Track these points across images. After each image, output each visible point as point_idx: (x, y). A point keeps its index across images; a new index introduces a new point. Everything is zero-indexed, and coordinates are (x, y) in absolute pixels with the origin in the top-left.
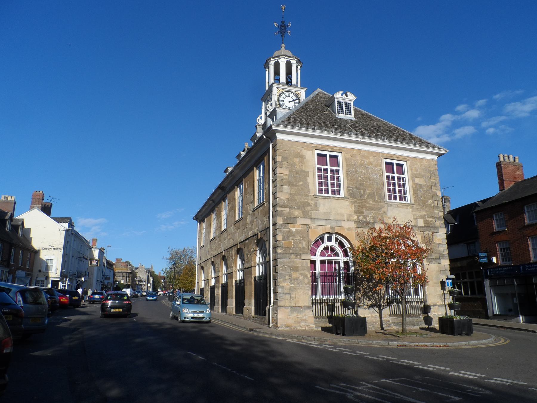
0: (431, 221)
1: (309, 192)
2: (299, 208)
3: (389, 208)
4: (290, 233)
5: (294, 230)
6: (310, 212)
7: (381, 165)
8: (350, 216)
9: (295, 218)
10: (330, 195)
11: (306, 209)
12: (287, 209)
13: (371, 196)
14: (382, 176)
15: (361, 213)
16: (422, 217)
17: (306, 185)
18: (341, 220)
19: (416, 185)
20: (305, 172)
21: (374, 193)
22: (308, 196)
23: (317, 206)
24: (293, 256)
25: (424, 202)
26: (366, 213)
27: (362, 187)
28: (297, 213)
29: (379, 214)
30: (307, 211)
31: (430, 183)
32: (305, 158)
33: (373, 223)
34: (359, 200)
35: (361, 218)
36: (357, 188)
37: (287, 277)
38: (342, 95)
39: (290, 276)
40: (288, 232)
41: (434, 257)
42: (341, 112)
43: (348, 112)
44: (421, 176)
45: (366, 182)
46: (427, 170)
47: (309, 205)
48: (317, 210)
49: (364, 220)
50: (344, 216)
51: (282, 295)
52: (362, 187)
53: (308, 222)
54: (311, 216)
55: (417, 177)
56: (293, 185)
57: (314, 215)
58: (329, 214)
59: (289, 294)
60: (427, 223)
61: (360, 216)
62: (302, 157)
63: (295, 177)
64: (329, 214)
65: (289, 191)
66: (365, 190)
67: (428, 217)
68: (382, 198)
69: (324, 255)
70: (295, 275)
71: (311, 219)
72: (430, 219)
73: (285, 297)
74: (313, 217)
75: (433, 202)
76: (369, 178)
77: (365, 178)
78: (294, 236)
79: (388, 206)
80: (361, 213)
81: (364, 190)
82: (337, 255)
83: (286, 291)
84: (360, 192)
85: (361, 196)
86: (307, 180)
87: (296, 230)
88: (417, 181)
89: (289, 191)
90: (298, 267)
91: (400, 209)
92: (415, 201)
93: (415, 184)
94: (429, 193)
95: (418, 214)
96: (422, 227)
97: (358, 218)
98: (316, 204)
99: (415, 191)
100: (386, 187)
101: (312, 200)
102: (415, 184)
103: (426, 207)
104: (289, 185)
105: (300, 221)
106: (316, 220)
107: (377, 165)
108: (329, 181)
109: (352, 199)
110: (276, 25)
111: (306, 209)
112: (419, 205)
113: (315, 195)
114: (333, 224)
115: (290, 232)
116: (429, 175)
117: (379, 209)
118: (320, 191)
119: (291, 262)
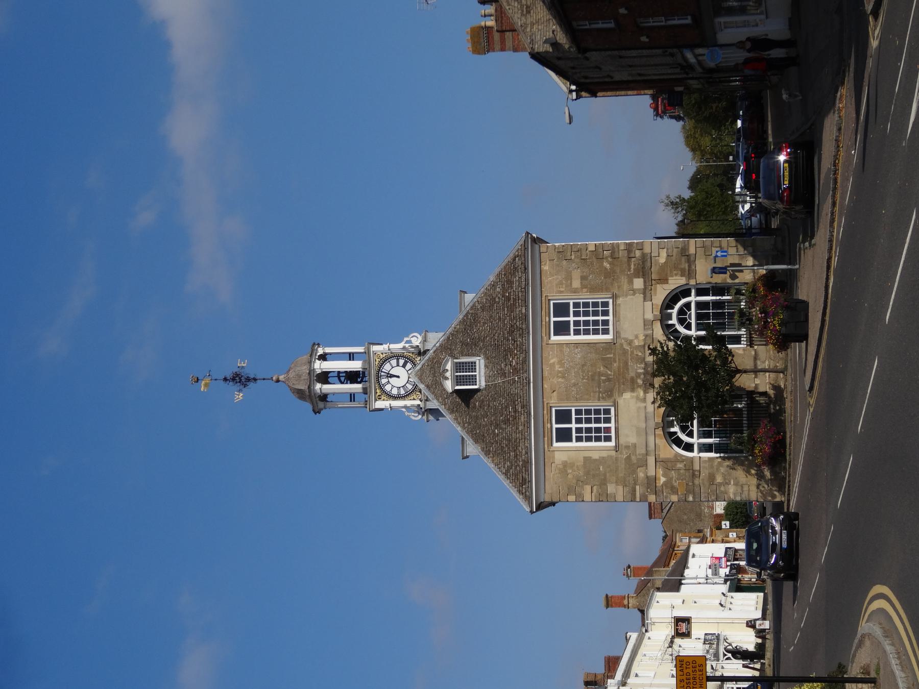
1: (611, 457)
2: (634, 472)
3: (623, 335)
5: (663, 480)
7: (560, 345)
8: (638, 398)
9: (647, 477)
10: (612, 425)
12: (638, 487)
13: (607, 363)
14: (577, 345)
15: (633, 381)
16: (631, 282)
17: (602, 460)
19: (583, 286)
21: (603, 359)
22: (617, 459)
24: (697, 482)
25: (608, 274)
27: (597, 378)
28: (641, 475)
29: (632, 352)
30: (638, 460)
31: (578, 260)
32: (566, 462)
33: (646, 364)
35: (640, 382)
36: (599, 387)
37: (722, 489)
38: (447, 378)
39: (720, 484)
40: (667, 487)
41: (687, 265)
42: (472, 380)
43: (472, 366)
44: (569, 277)
45: (588, 371)
46: (558, 265)
47: (629, 458)
48: (635, 446)
49: (642, 376)
50: (639, 408)
51: (743, 496)
52: (597, 378)
53: (651, 460)
55: (571, 284)
56: (605, 479)
57: (641, 450)
58: (638, 429)
59: (742, 487)
62: (565, 464)
63: (594, 476)
64: (638, 429)
67: (629, 270)
68: (609, 346)
69: (692, 431)
70: (719, 479)
72: (632, 266)
73: (746, 493)
74: (644, 451)
75: (607, 258)
76: (583, 366)
77: (583, 372)
80: (633, 381)
81: (600, 374)
83: (739, 490)
84: (604, 381)
85: (609, 380)
87: (663, 476)
88: (576, 284)
89: (614, 485)
91: (621, 319)
92: (607, 290)
93: (582, 288)
94: (592, 263)
95: (626, 287)
96: (645, 282)
97: (639, 386)
98: (627, 447)
99: (593, 289)
100: (591, 337)
101: (621, 453)
102: (582, 288)
103: (614, 272)
104: (605, 484)
105: (651, 473)
106: (649, 449)
108: (593, 425)
109: (616, 394)
112: (612, 284)
113: (617, 448)
114: (652, 424)
115: (665, 484)
116: (564, 262)
117: (625, 352)
118: (608, 439)
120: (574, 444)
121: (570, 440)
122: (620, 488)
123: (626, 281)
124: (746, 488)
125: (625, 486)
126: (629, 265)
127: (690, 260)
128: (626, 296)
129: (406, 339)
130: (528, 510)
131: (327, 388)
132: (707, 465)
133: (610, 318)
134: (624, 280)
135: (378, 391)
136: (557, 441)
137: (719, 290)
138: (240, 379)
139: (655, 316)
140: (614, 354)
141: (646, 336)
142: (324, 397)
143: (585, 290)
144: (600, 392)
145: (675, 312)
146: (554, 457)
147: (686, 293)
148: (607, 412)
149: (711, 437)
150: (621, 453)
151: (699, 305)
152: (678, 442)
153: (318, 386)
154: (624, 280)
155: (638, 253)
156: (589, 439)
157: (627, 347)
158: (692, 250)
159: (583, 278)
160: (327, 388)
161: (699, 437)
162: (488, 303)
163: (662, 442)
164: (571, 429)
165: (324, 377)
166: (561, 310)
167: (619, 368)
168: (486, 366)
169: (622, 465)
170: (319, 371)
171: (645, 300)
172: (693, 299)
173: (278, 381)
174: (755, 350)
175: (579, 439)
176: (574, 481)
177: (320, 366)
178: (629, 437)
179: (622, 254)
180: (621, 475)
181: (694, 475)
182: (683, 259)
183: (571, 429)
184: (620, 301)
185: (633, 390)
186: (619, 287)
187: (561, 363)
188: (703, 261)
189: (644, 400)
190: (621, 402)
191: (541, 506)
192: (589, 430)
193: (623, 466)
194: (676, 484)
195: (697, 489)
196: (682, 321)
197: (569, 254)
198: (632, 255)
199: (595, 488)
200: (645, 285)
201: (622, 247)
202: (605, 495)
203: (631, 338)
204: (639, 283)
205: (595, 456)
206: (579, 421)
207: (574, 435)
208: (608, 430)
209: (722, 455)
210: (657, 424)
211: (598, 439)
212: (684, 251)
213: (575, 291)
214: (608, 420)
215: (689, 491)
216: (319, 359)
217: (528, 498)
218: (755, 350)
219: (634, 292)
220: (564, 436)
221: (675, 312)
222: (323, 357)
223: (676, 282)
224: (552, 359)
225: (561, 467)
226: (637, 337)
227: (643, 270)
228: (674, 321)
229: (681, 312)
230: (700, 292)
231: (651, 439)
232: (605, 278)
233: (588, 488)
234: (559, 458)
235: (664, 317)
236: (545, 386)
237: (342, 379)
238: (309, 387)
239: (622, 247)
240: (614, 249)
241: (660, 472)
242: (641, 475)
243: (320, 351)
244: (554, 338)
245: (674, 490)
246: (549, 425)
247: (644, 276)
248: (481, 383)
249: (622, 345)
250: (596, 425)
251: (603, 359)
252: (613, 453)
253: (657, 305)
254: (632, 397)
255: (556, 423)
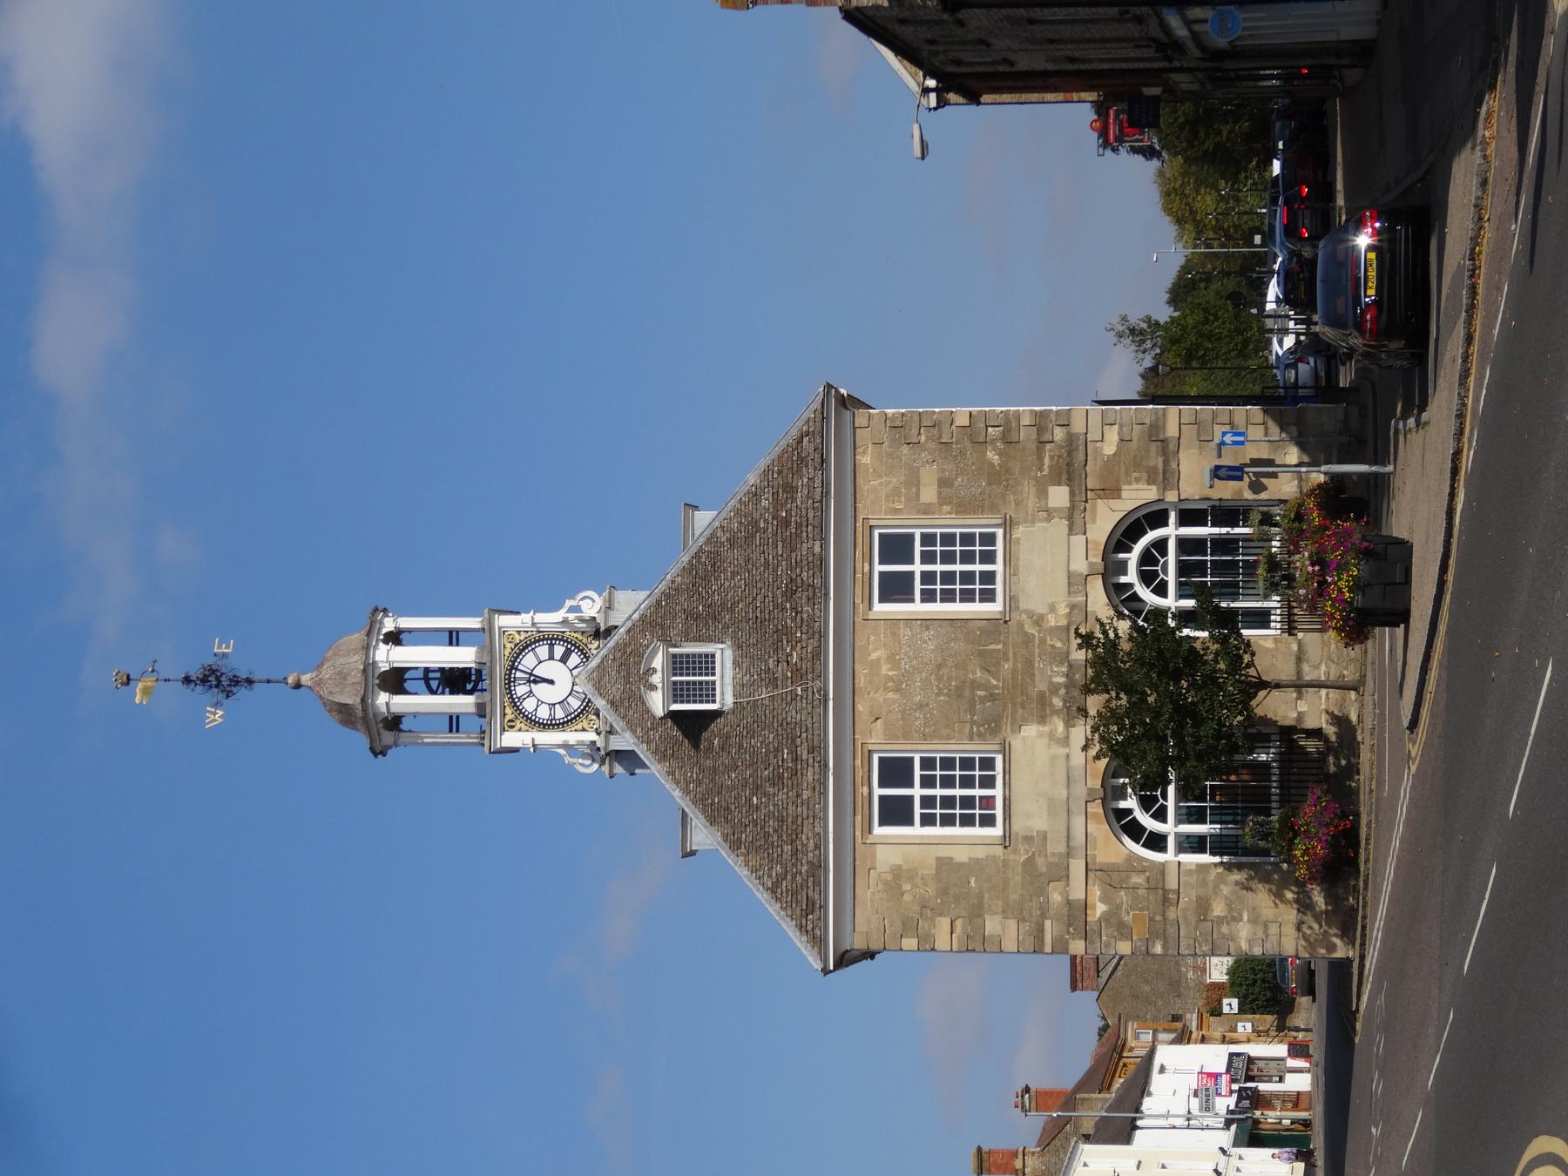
0: (1051, 458)
1: (994, 858)
2: (1042, 891)
3: (1023, 605)
4: (1113, 919)
5: (1100, 908)
6: (1051, 860)
7: (892, 622)
9: (1069, 903)
10: (997, 792)
11: (1044, 869)
12: (1048, 923)
13: (990, 663)
14: (927, 622)
15: (1043, 701)
16: (1043, 494)
17: (976, 866)
18: (1068, 769)
19: (943, 500)
20: (938, 868)
21: (982, 654)
22: (1005, 863)
23: (1032, 838)
24: (1172, 914)
26: (1042, 686)
27: (967, 693)
28: (1056, 897)
29: (1043, 641)
30: (1050, 865)
31: (932, 445)
32: (899, 867)
33: (1070, 666)
34: (1005, 705)
35: (1058, 702)
36: (972, 710)
37: (1225, 929)
38: (653, 688)
39: (1221, 920)
40: (1107, 921)
41: (1160, 460)
42: (707, 692)
44: (914, 482)
45: (950, 679)
46: (890, 455)
47: (1030, 862)
48: (1044, 836)
49: (1062, 691)
50: (1054, 758)
51: (1268, 946)
52: (967, 693)
53: (1077, 867)
54: (1060, 854)
55: (918, 495)
56: (980, 905)
57: (1056, 846)
58: (1051, 802)
59: (1266, 927)
60: (1060, 474)
61: (1052, 705)
62: (897, 873)
63: (957, 898)
65: (998, 918)
66: (973, 681)
67: (1041, 469)
69: (1163, 809)
70: (1218, 909)
71: (1068, 855)
72: (1047, 461)
73: (1273, 939)
74: (1062, 849)
76: (939, 666)
77: (939, 679)
78: (1119, 907)
79: (1018, 608)
80: (1043, 701)
81: (975, 685)
82: (1161, 545)
83: (1260, 934)
84: (982, 700)
85: (992, 697)
86: (962, 865)
87: (1102, 900)
88: (929, 494)
89: (998, 918)
90: (1199, 898)
92: (993, 509)
93: (941, 505)
94: (962, 453)
95: (1032, 502)
96: (1072, 494)
97: (1057, 713)
98: (1028, 839)
99: (963, 508)
101: (1016, 851)
103: (1008, 471)
104: (980, 916)
105: (1077, 893)
106: (1074, 844)
107: (893, 634)
108: (958, 792)
109: (1007, 728)
110: (216, 717)
111: (1044, 869)
112: (1004, 497)
113: (1006, 841)
114: (1080, 791)
115: (1105, 917)
116: (905, 449)
117: (1028, 640)
118: (988, 821)
119: (1186, 919)
120: (917, 830)
121: (910, 822)
122: (1012, 924)
123: (1033, 490)
124: (1273, 929)
125: (1021, 920)
126: (1041, 459)
127: (1168, 450)
128: (1033, 522)
129: (569, 603)
130: (818, 966)
131: (400, 703)
132: (1193, 880)
133: (998, 567)
134: (1029, 490)
135: (508, 710)
136: (881, 824)
137: (1227, 514)
138: (217, 680)
139: (1091, 565)
140: (1005, 644)
141: (1073, 607)
142: (394, 722)
143: (946, 508)
144: (973, 723)
145: (1133, 557)
146: (874, 857)
147: (1158, 519)
148: (988, 764)
149: (1203, 822)
150: (1016, 851)
151: (1185, 545)
152: (1135, 831)
153: (383, 698)
154: (1029, 490)
155: (1059, 434)
156: (948, 821)
157: (1033, 631)
158: (1172, 430)
159: (943, 483)
160: (400, 703)
161: (1179, 821)
162: (743, 531)
163: (1101, 830)
164: (911, 798)
165: (396, 680)
166: (897, 548)
167: (1014, 671)
168: (736, 664)
169: (1016, 878)
170: (384, 667)
171: (1071, 531)
172: (1171, 531)
173: (298, 686)
174: (1300, 643)
175: (928, 820)
176: (917, 908)
177: (387, 656)
178: (1033, 817)
179: (1026, 435)
180: (1014, 897)
181: (1165, 901)
182: (1154, 447)
183: (911, 798)
184: (1019, 532)
185: (1042, 720)
186: (1017, 504)
187: (893, 659)
188: (1195, 451)
189: (1066, 741)
190: (1016, 743)
191: (845, 960)
192: (948, 802)
193: (1018, 878)
194: (1128, 919)
195: (1171, 931)
196: (1147, 578)
197: (915, 432)
198: (1047, 437)
199: (959, 924)
200: (1072, 500)
201: (1026, 421)
202: (979, 938)
203: (1040, 609)
204: (1059, 496)
205: (961, 855)
206: (927, 782)
207: (917, 811)
208: (988, 802)
209: (1226, 859)
210: (1091, 791)
211: (967, 821)
212: (1155, 432)
213: (926, 510)
214: (988, 782)
215: (1154, 934)
216: (386, 641)
217: (818, 942)
218: (1300, 643)
219: (1050, 514)
220: (896, 812)
221: (1133, 557)
222: (395, 638)
223: (1138, 495)
224: (874, 652)
225: (889, 877)
226: (1053, 608)
227: (1069, 469)
228: (1131, 577)
229: (1147, 558)
230: (1189, 517)
231: (1078, 822)
232: (989, 484)
233: (944, 923)
234: (886, 858)
235: (1111, 569)
236: (859, 707)
237: (434, 684)
238: (363, 700)
239: (1026, 421)
240: (1008, 424)
241: (1096, 891)
242: (1056, 897)
243: (389, 625)
244: (881, 609)
245: (1124, 931)
246: (865, 790)
247: (1070, 481)
248: (725, 698)
249: (1021, 625)
250: (963, 788)
251: (982, 654)
252: (999, 851)
253: (1096, 543)
254: (1041, 735)
255: (881, 785)
